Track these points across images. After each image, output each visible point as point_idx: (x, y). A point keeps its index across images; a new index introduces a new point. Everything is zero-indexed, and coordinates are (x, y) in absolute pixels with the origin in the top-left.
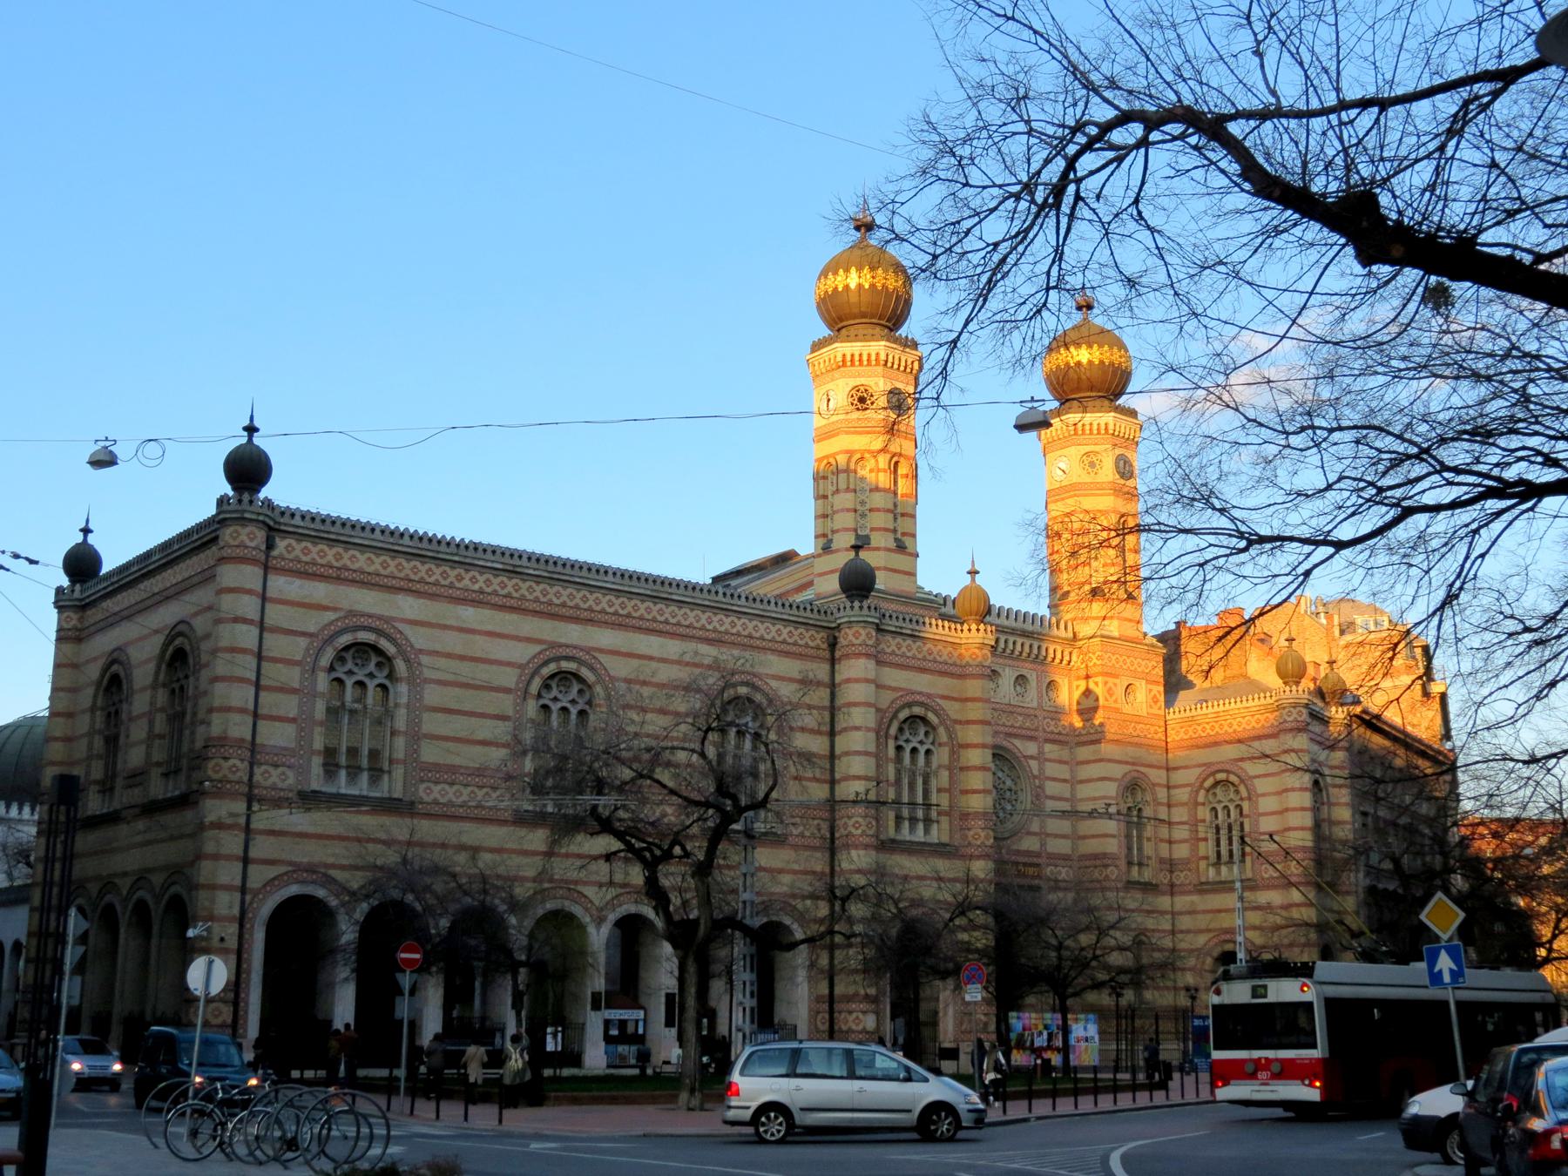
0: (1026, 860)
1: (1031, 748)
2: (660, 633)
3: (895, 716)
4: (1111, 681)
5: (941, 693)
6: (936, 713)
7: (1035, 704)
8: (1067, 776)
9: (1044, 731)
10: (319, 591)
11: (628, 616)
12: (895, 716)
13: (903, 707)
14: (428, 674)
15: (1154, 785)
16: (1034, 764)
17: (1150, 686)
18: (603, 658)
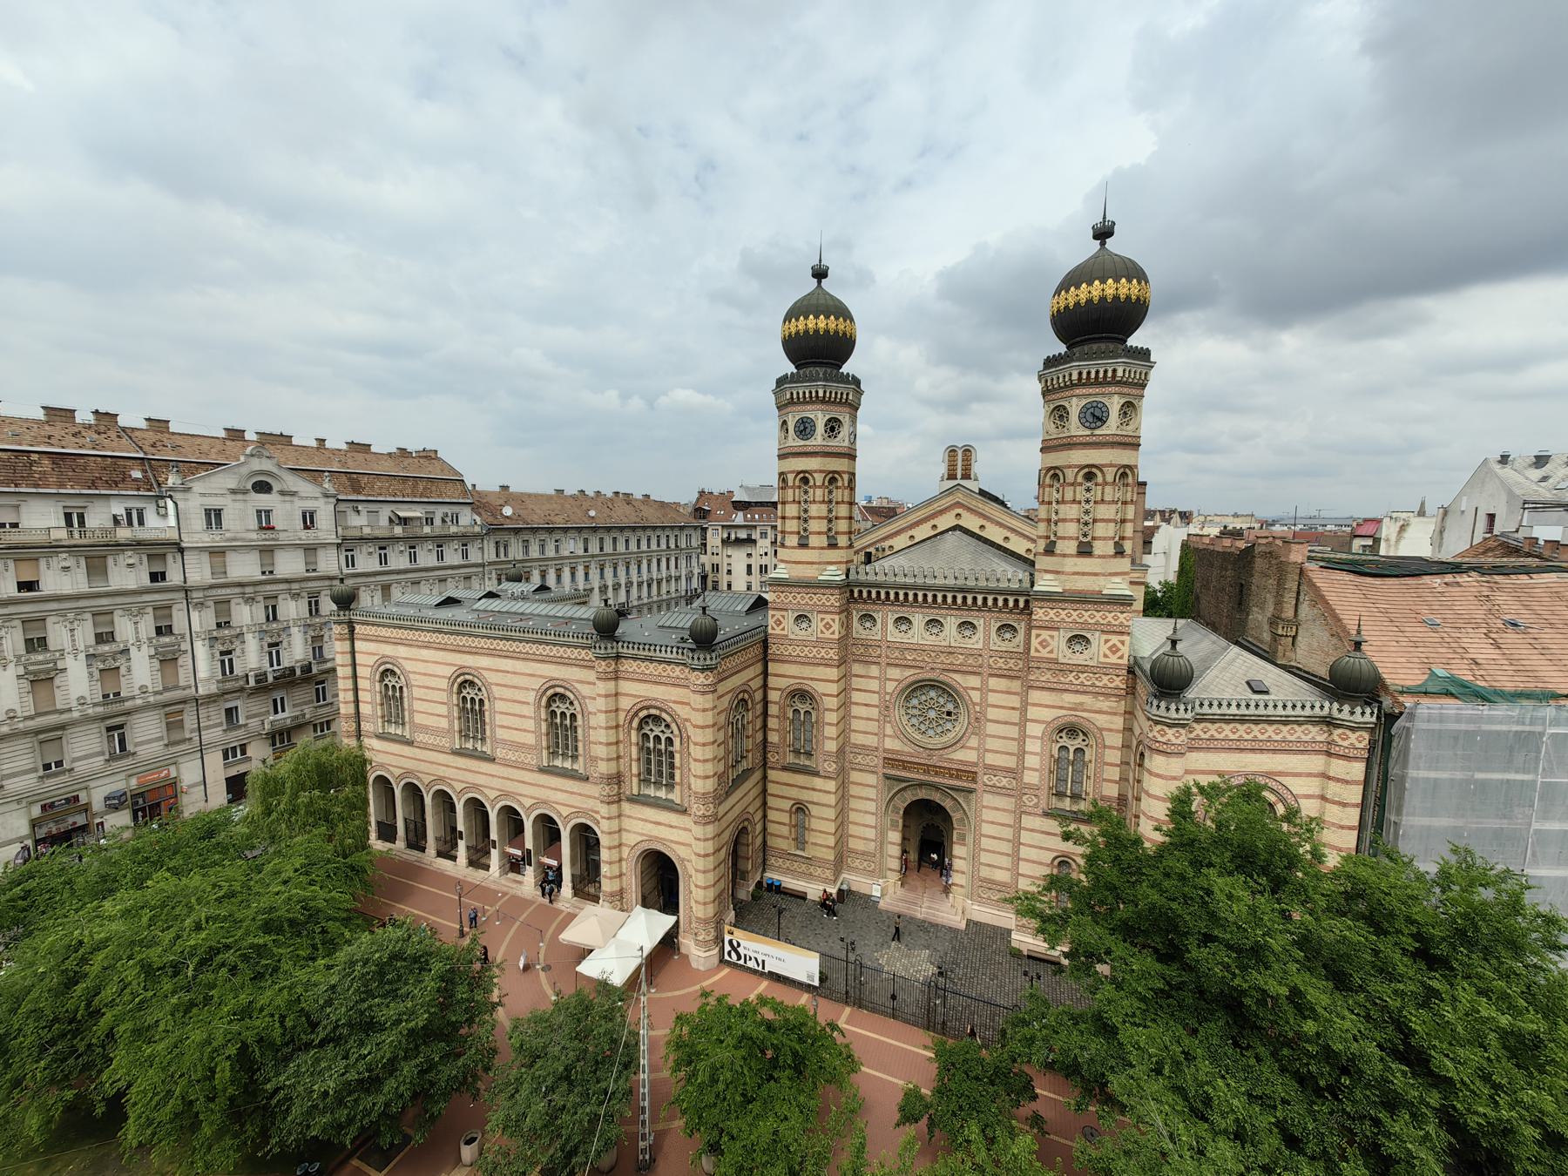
0: (960, 767)
1: (974, 681)
2: (512, 658)
3: (636, 714)
4: (1045, 634)
5: (673, 699)
6: (668, 714)
7: (980, 646)
8: (1018, 705)
9: (990, 667)
10: (371, 647)
11: (495, 649)
12: (636, 714)
13: (641, 709)
14: (413, 683)
15: (1101, 730)
16: (976, 696)
17: (1105, 637)
18: (485, 673)
